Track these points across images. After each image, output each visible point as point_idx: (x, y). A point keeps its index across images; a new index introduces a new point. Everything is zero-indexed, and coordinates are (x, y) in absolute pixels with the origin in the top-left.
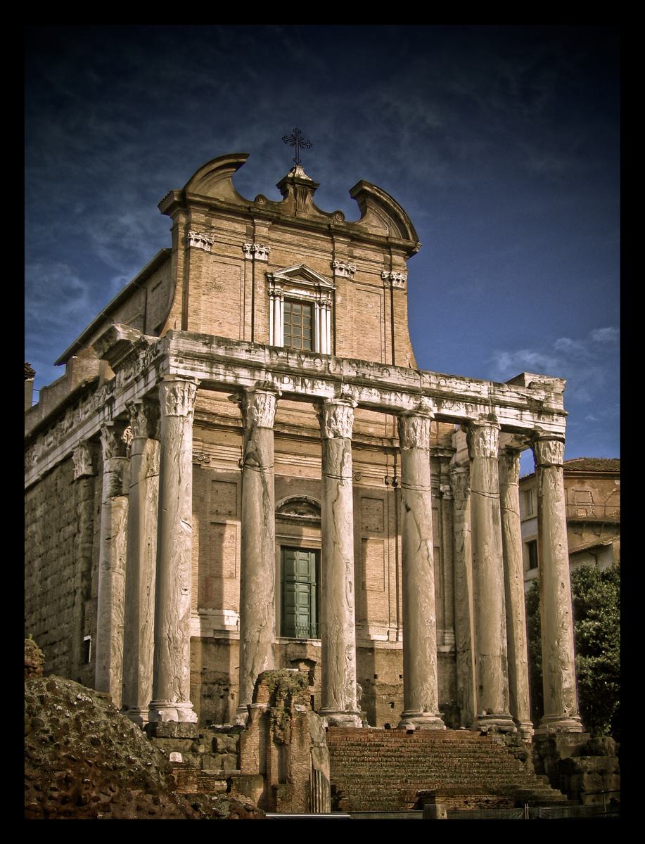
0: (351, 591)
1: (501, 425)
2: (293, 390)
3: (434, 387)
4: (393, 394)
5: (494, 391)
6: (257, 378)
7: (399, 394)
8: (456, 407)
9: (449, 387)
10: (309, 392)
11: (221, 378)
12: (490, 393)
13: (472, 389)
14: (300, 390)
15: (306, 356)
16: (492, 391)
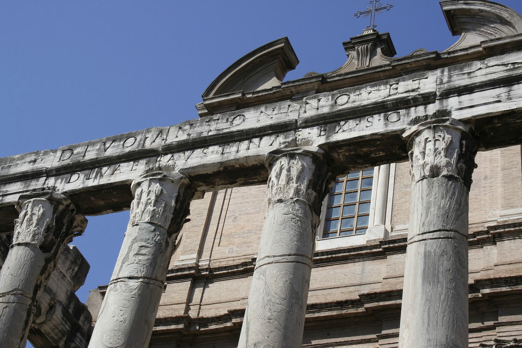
1: (465, 122)
2: (81, 186)
3: (326, 110)
4: (246, 142)
5: (450, 77)
6: (31, 188)
7: (256, 140)
8: (364, 123)
9: (354, 102)
10: (104, 181)
12: (441, 83)
13: (400, 90)
14: (91, 183)
15: (114, 141)
16: (445, 79)
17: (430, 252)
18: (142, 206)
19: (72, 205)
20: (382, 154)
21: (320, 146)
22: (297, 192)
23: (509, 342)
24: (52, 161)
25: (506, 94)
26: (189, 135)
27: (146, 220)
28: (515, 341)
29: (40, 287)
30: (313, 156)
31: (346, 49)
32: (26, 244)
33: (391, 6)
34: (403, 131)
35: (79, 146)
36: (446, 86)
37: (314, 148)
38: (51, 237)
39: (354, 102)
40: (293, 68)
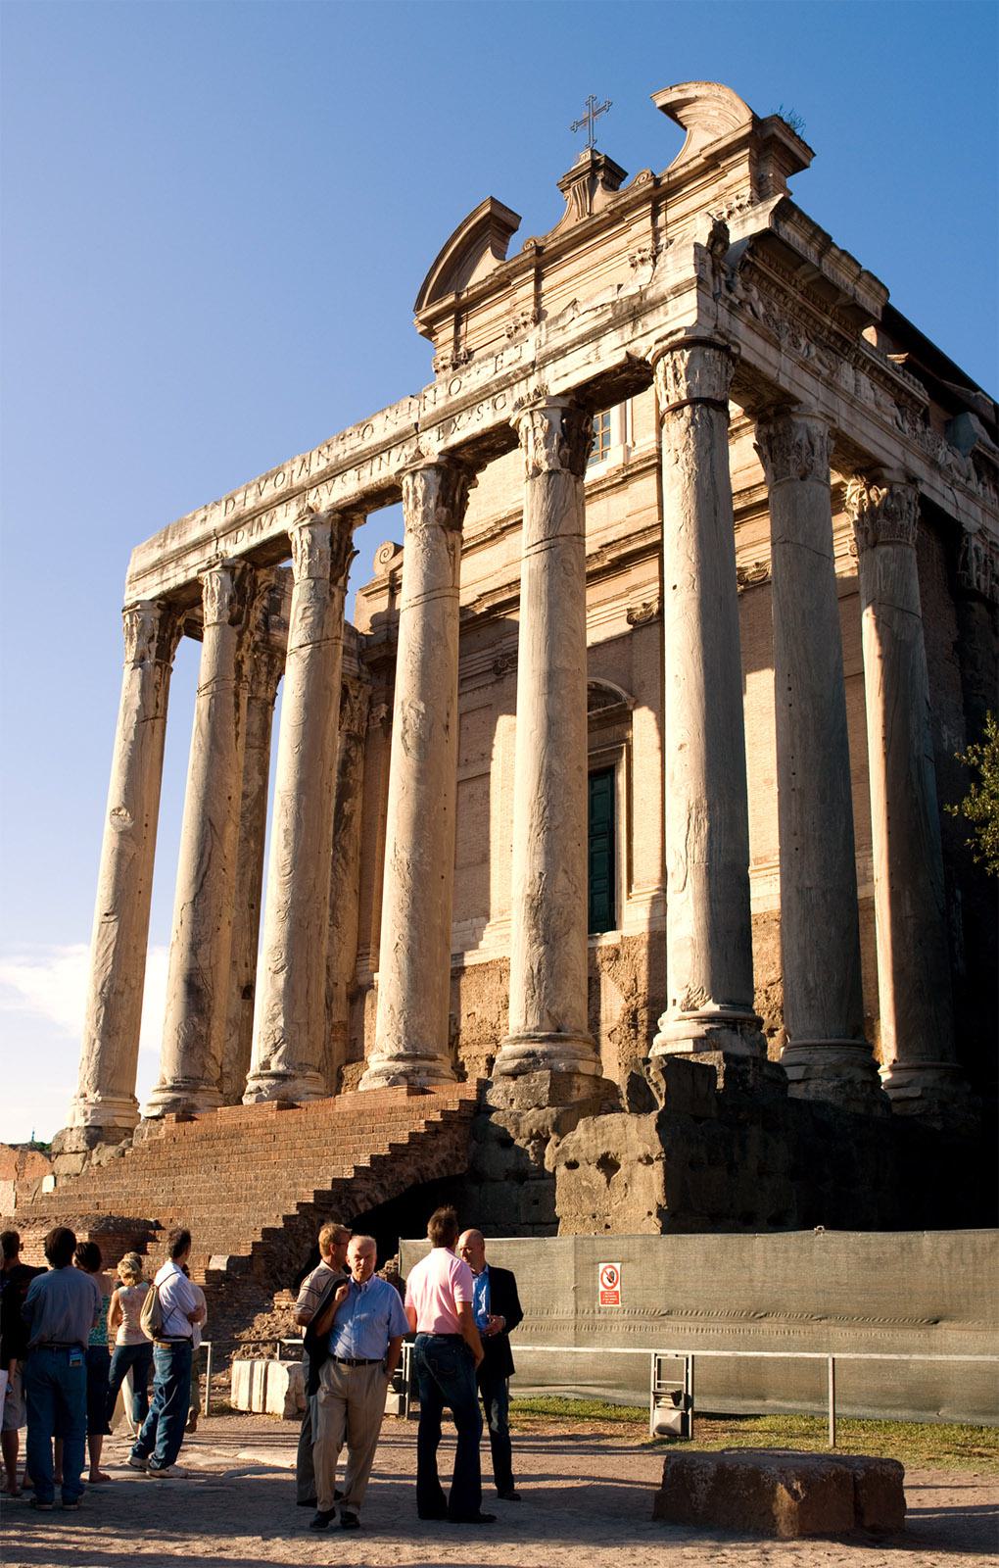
0: (285, 847)
1: (564, 394)
3: (441, 404)
5: (547, 336)
6: (207, 556)
7: (385, 456)
9: (465, 387)
11: (171, 584)
13: (505, 363)
17: (533, 570)
18: (299, 560)
19: (248, 564)
20: (505, 443)
21: (440, 454)
22: (425, 515)
23: (750, 568)
24: (218, 518)
25: (595, 352)
26: (328, 460)
27: (305, 577)
28: (757, 564)
29: (243, 661)
30: (434, 467)
31: (562, 191)
32: (215, 624)
33: (611, 104)
34: (509, 419)
35: (236, 494)
36: (543, 350)
37: (433, 458)
38: (237, 607)
39: (465, 387)
40: (514, 230)
